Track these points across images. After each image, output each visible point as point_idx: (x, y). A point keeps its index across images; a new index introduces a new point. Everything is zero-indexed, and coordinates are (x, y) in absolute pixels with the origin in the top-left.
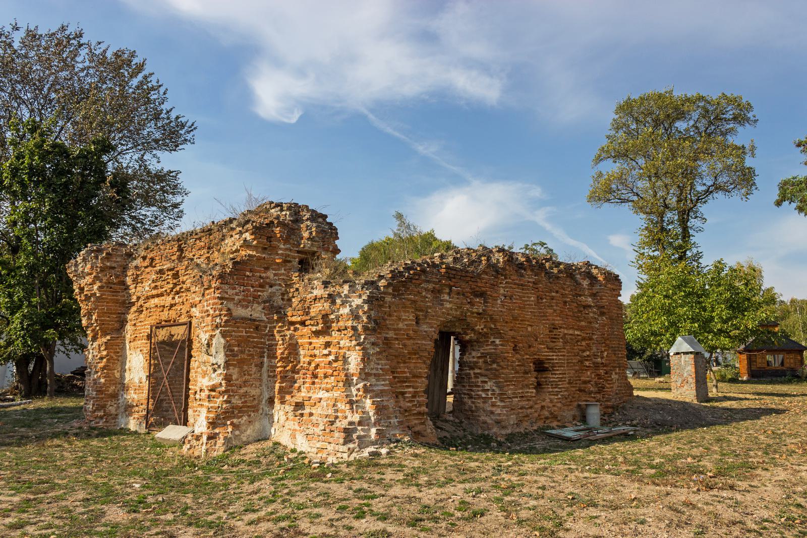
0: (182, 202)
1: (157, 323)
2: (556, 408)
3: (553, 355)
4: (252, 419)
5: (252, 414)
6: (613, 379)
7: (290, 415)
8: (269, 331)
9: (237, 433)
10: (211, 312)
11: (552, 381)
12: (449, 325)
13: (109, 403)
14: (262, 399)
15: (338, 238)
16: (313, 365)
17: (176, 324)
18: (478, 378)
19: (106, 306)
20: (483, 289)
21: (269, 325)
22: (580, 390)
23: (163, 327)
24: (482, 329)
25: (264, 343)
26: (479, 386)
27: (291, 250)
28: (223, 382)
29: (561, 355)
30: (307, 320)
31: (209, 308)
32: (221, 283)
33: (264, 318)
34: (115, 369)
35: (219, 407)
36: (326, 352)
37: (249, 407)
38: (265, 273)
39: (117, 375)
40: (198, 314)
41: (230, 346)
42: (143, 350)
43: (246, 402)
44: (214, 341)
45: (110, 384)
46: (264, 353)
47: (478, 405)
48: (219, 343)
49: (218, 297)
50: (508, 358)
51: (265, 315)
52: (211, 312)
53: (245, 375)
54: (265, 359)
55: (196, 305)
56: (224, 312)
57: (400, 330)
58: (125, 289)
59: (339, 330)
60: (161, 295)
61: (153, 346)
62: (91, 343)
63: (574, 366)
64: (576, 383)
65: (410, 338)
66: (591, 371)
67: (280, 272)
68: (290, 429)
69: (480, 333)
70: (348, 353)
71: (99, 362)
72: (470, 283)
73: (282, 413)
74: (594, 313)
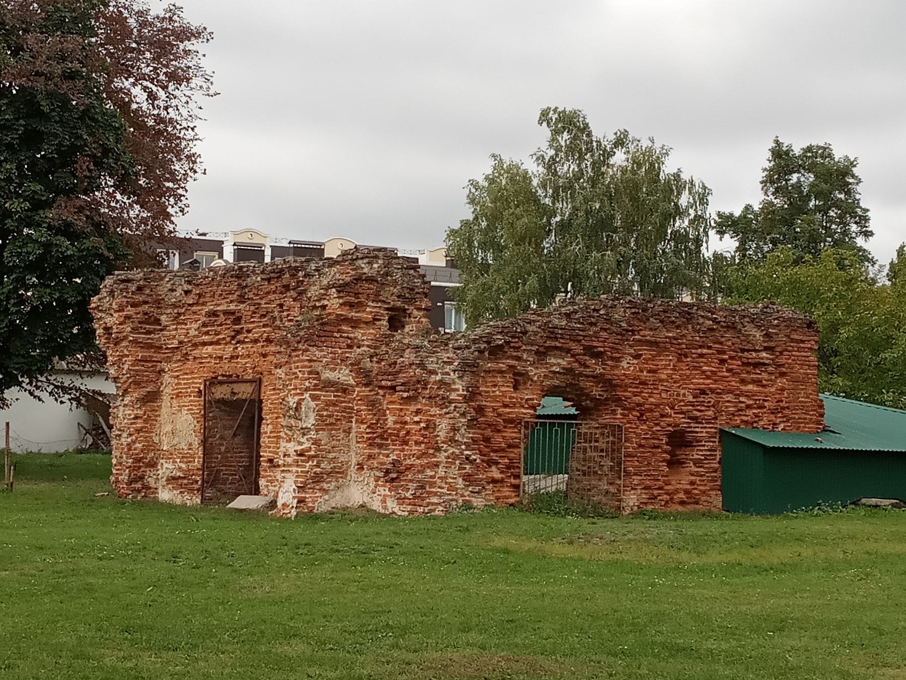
1: (212, 378)
2: (696, 492)
3: (695, 427)
14: (351, 465)
16: (403, 433)
17: (239, 380)
20: (602, 349)
21: (357, 389)
23: (221, 383)
29: (710, 428)
31: (297, 371)
36: (416, 419)
38: (353, 333)
40: (283, 376)
43: (335, 467)
52: (300, 375)
53: (333, 440)
60: (217, 343)
62: (121, 398)
74: (770, 374)
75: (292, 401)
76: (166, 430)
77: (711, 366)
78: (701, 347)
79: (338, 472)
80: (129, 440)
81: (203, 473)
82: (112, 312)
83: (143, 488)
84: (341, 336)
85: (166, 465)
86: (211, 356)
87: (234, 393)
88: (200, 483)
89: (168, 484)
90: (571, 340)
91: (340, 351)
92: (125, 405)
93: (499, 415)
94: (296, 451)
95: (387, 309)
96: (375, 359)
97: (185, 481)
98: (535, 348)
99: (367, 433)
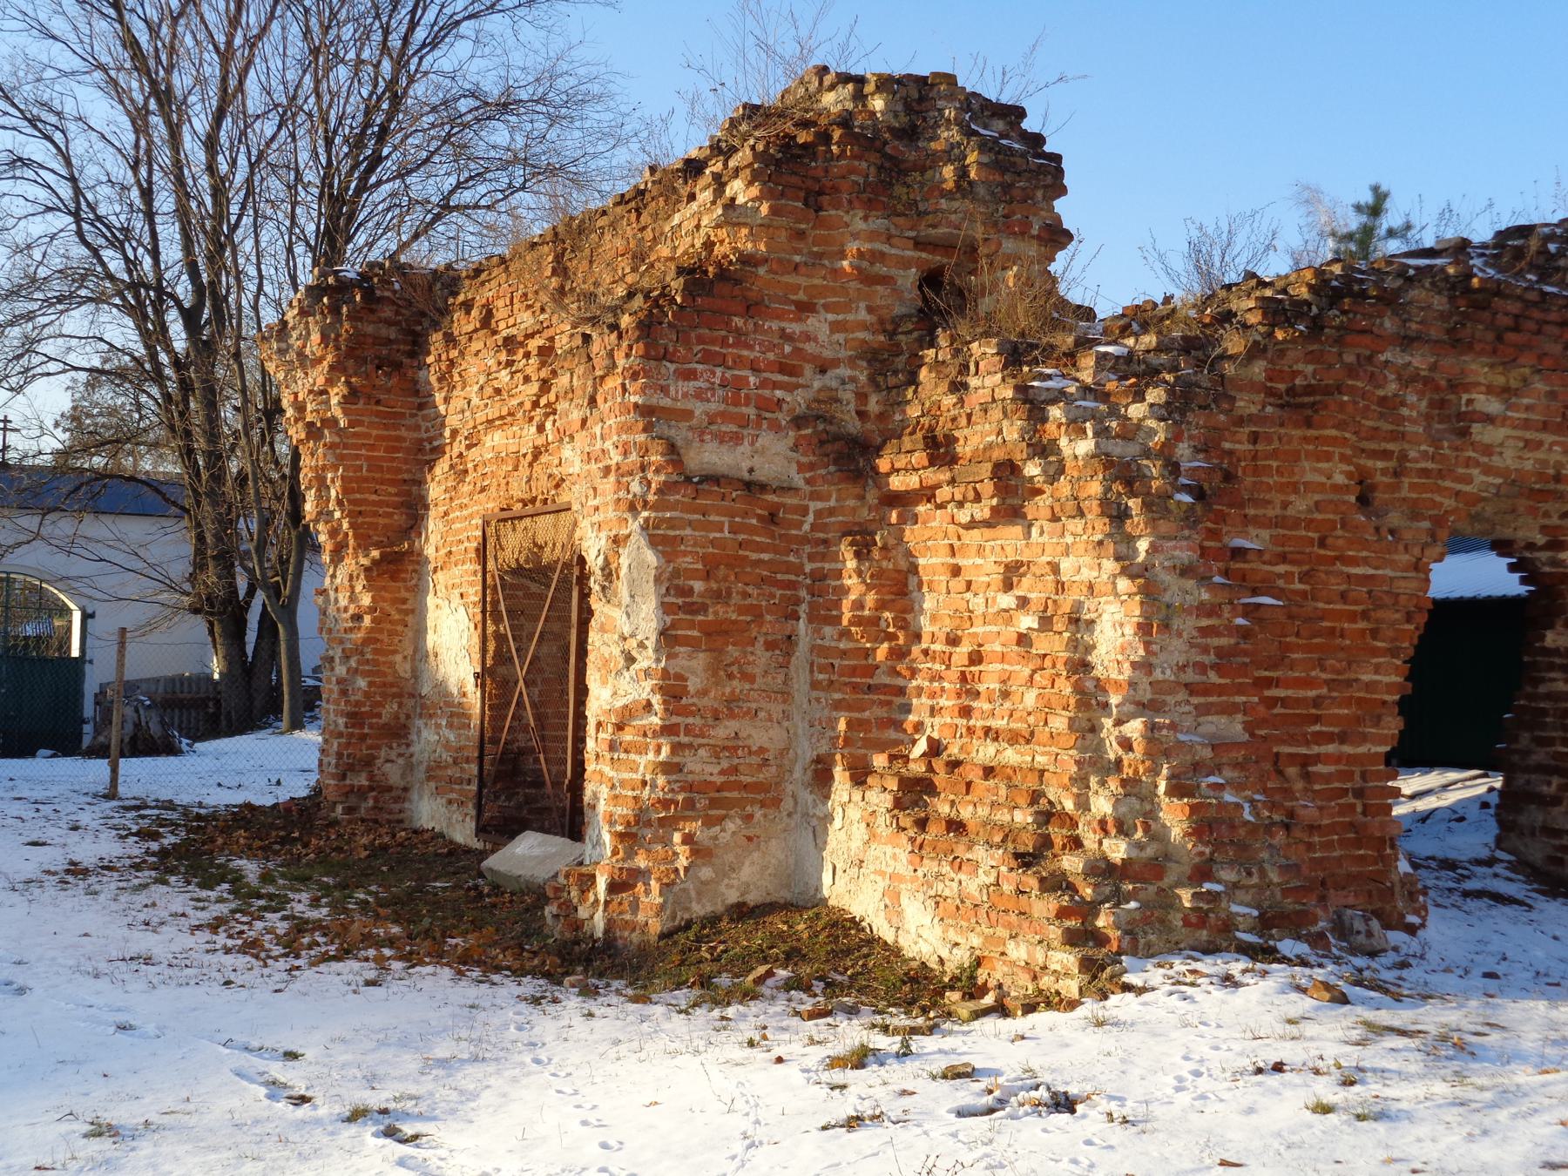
1: (502, 510)
4: (757, 831)
5: (758, 814)
7: (882, 820)
8: (814, 527)
9: (706, 873)
10: (615, 457)
13: (383, 753)
15: (1063, 191)
16: (964, 649)
19: (368, 458)
21: (814, 506)
25: (799, 569)
27: (889, 239)
28: (656, 700)
30: (939, 486)
32: (646, 356)
33: (798, 480)
34: (395, 652)
35: (644, 783)
37: (746, 787)
38: (799, 320)
39: (404, 669)
41: (676, 573)
43: (735, 770)
48: (642, 564)
49: (636, 405)
51: (801, 468)
53: (730, 676)
54: (802, 624)
55: (572, 437)
56: (656, 458)
58: (421, 407)
61: (489, 580)
67: (850, 317)
68: (882, 873)
70: (1090, 604)
71: (351, 630)
73: (854, 813)
83: (371, 789)
85: (425, 734)
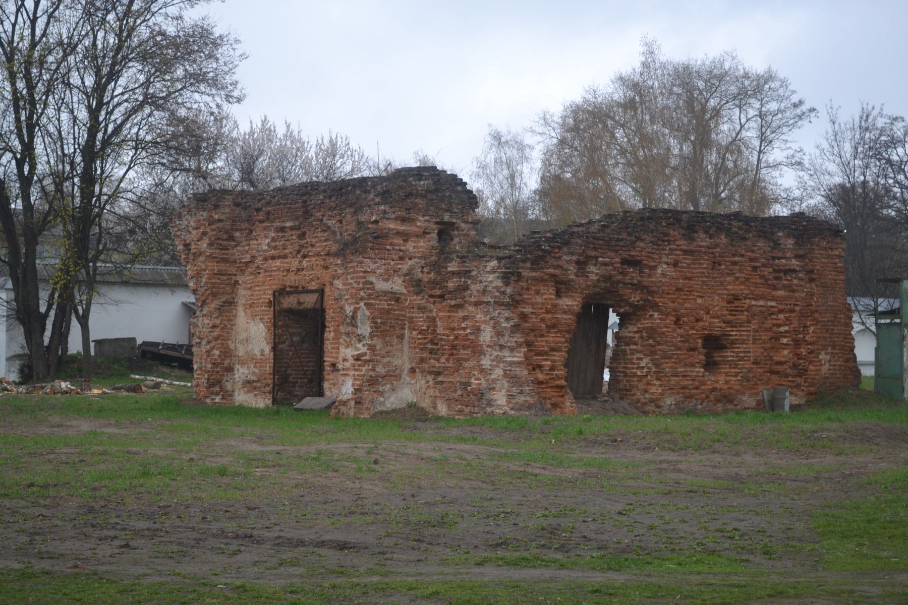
0: (288, 126)
6: (820, 360)
11: (730, 361)
12: (598, 297)
16: (452, 338)
18: (634, 354)
20: (639, 258)
21: (409, 298)
22: (772, 372)
23: (290, 293)
24: (638, 301)
25: (405, 316)
26: (634, 364)
29: (744, 331)
33: (405, 291)
36: (463, 325)
38: (404, 245)
40: (341, 286)
41: (373, 318)
42: (263, 319)
43: (389, 371)
44: (359, 314)
45: (225, 356)
46: (405, 325)
47: (632, 383)
50: (667, 334)
51: (405, 287)
57: (536, 303)
59: (475, 305)
60: (285, 257)
63: (764, 342)
64: (767, 364)
65: (548, 312)
66: (789, 351)
69: (637, 305)
72: (621, 252)
74: (800, 279)
75: (349, 310)
76: (241, 338)
77: (744, 273)
78: (734, 255)
79: (391, 376)
80: (208, 347)
81: (274, 377)
82: (190, 229)
84: (393, 249)
85: (241, 370)
86: (279, 270)
87: (299, 303)
88: (271, 386)
89: (243, 387)
90: (610, 250)
91: (392, 263)
92: (204, 315)
93: (543, 320)
94: (353, 356)
95: (437, 223)
96: (425, 270)
97: (259, 385)
98: (574, 258)
99: (419, 339)
